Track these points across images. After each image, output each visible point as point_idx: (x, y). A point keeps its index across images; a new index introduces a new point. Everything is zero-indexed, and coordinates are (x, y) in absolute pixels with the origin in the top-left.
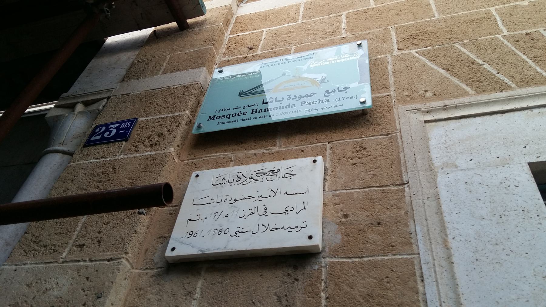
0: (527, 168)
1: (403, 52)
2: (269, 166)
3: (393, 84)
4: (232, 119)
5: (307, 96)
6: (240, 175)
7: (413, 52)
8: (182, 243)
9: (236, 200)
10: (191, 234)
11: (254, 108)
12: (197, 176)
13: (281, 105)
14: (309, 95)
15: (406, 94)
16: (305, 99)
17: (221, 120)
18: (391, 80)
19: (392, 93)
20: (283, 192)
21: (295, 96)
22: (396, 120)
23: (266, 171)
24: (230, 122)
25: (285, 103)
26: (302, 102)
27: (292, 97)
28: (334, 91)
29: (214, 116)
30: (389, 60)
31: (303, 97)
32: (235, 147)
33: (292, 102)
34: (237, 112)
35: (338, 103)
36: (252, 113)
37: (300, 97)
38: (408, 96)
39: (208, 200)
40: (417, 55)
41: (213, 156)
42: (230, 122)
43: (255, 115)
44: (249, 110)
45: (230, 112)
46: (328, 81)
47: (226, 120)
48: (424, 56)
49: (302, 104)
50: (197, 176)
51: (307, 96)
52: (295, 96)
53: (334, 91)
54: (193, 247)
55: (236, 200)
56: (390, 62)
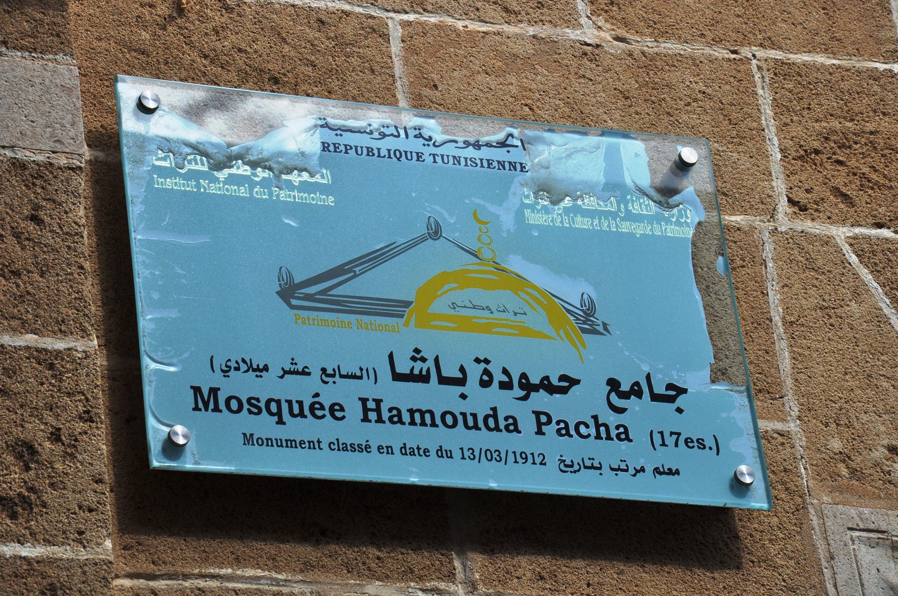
3: (789, 382)
5: (546, 385)
7: (841, 233)
13: (466, 407)
14: (555, 381)
15: (836, 444)
16: (541, 400)
18: (785, 363)
19: (793, 426)
21: (505, 371)
22: (824, 563)
25: (480, 400)
26: (537, 414)
27: (498, 377)
28: (636, 391)
29: (214, 391)
30: (769, 251)
31: (536, 388)
32: (306, 551)
36: (366, 419)
37: (528, 387)
38: (845, 458)
40: (854, 259)
41: (230, 578)
42: (291, 443)
46: (605, 325)
47: (264, 425)
48: (876, 272)
49: (539, 424)
51: (546, 385)
52: (505, 371)
53: (636, 391)
56: (770, 264)
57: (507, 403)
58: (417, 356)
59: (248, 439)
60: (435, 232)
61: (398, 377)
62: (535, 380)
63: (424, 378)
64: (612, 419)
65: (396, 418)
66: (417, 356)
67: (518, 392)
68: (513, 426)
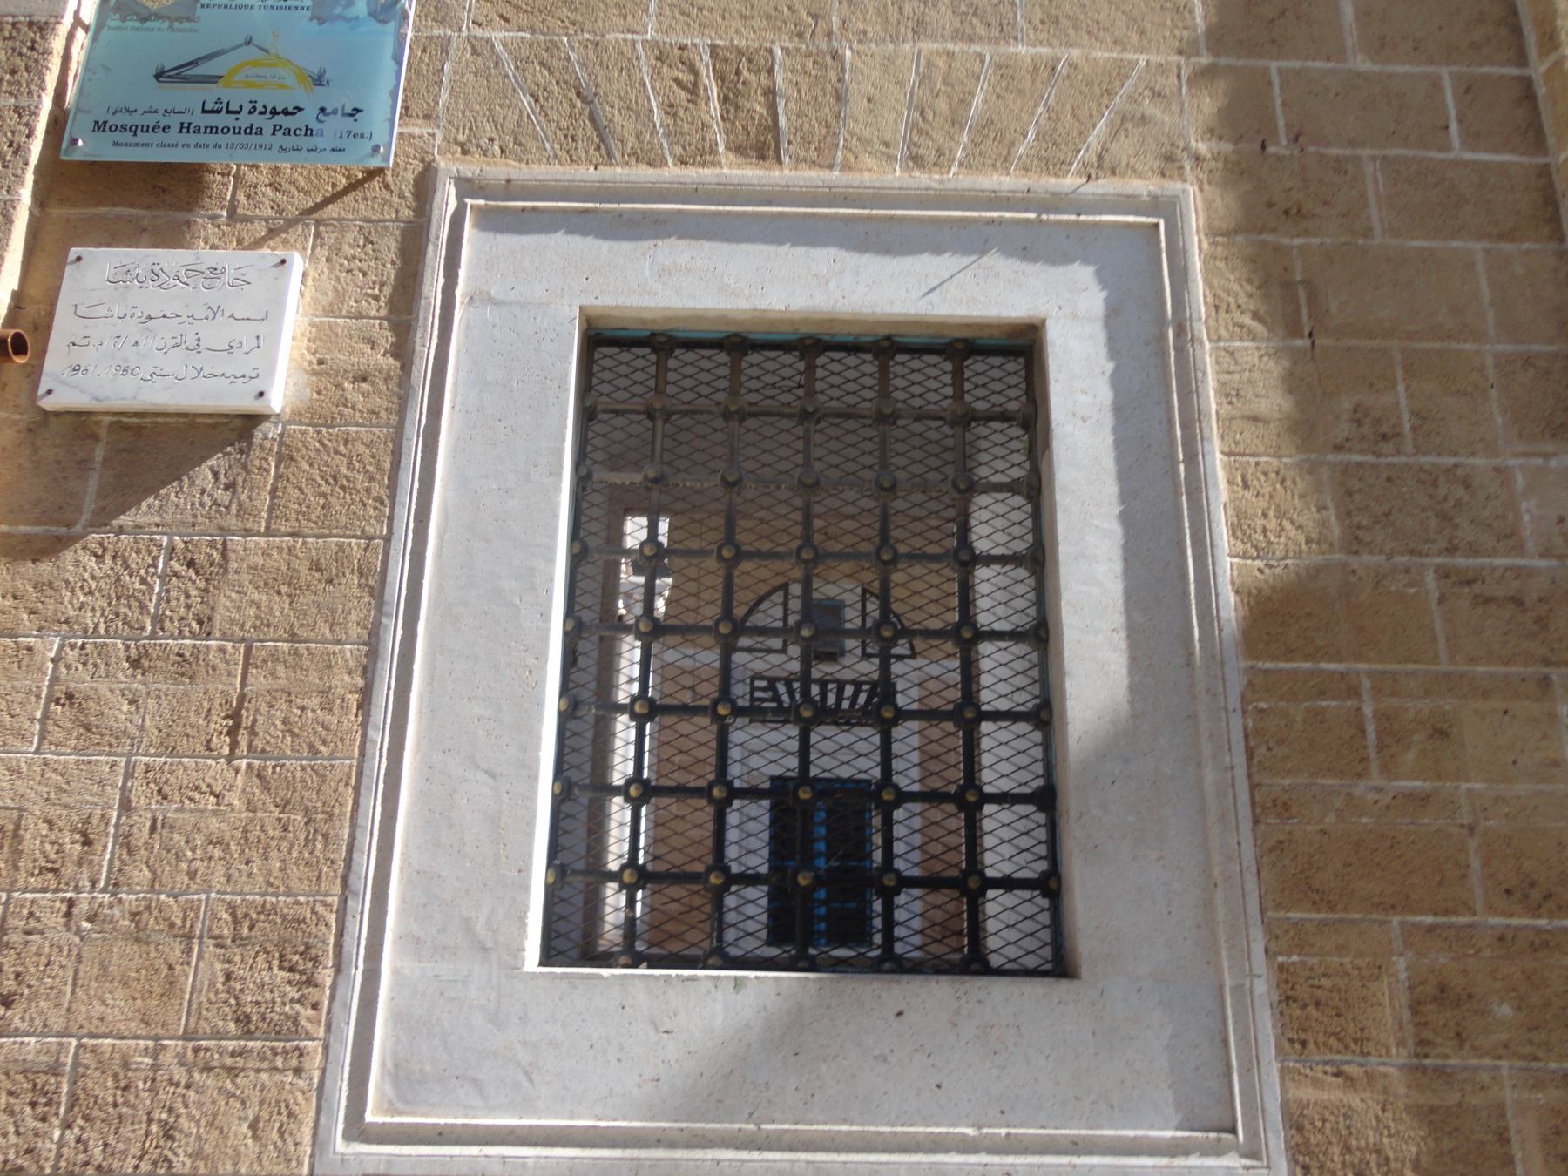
4: (142, 137)
5: (286, 112)
6: (156, 268)
8: (63, 382)
9: (150, 318)
11: (186, 118)
12: (79, 259)
13: (237, 124)
16: (279, 119)
17: (118, 136)
20: (227, 314)
23: (203, 268)
24: (137, 145)
25: (245, 120)
27: (259, 108)
28: (335, 112)
33: (258, 120)
34: (150, 120)
35: (339, 144)
37: (274, 112)
42: (137, 145)
44: (174, 122)
45: (137, 119)
50: (79, 259)
51: (286, 112)
53: (335, 112)
54: (82, 391)
55: (150, 318)
58: (219, 101)
59: (116, 144)
60: (248, 42)
61: (204, 111)
62: (279, 109)
63: (218, 112)
66: (219, 101)
67: (268, 115)
68: (260, 132)
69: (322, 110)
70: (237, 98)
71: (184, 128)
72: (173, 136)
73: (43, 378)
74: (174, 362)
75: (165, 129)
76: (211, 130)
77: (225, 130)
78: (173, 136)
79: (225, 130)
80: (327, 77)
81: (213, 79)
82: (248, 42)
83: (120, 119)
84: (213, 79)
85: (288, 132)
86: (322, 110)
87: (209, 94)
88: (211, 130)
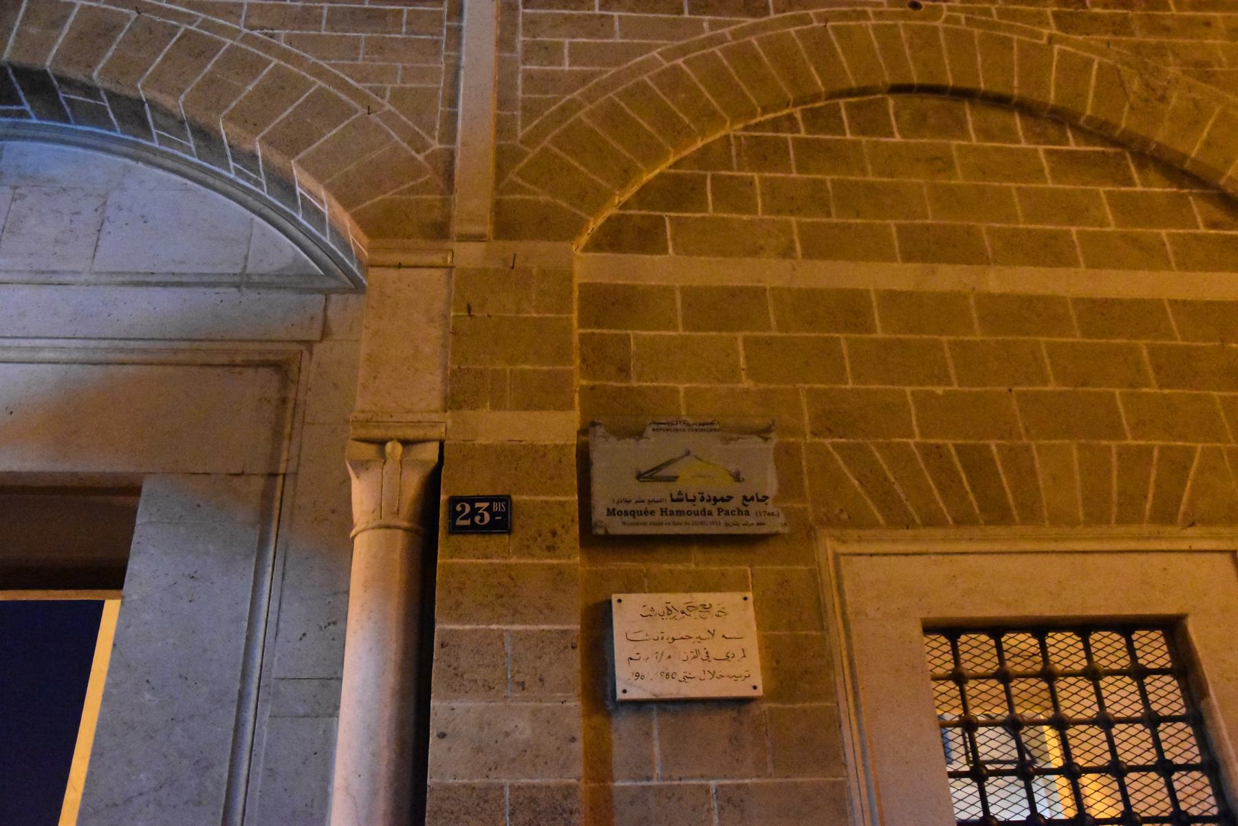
0: (919, 623)
1: (817, 440)
2: (700, 598)
5: (722, 500)
10: (637, 675)
12: (620, 601)
13: (695, 508)
16: (720, 504)
25: (700, 506)
28: (752, 499)
34: (641, 507)
35: (760, 519)
37: (716, 500)
39: (641, 636)
43: (665, 519)
47: (629, 519)
51: (722, 500)
53: (752, 499)
57: (709, 506)
58: (680, 493)
60: (688, 453)
61: (673, 500)
63: (681, 500)
64: (744, 509)
65: (672, 513)
66: (680, 493)
68: (710, 514)
69: (745, 498)
70: (692, 489)
71: (663, 512)
72: (657, 517)
73: (618, 683)
74: (696, 667)
75: (652, 513)
76: (680, 513)
77: (689, 513)
78: (657, 517)
79: (689, 513)
80: (742, 476)
81: (673, 479)
82: (688, 453)
83: (622, 507)
84: (673, 479)
85: (727, 513)
86: (745, 498)
87: (674, 488)
88: (680, 513)
